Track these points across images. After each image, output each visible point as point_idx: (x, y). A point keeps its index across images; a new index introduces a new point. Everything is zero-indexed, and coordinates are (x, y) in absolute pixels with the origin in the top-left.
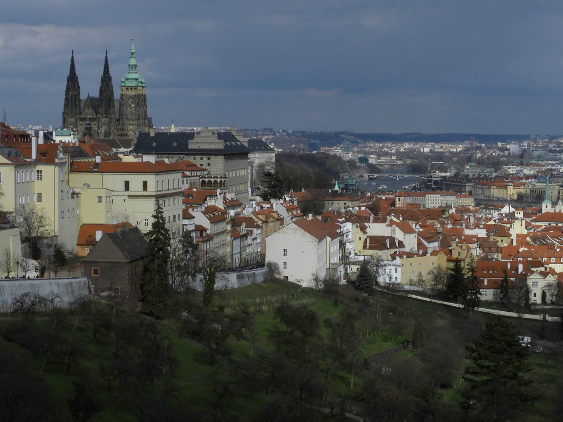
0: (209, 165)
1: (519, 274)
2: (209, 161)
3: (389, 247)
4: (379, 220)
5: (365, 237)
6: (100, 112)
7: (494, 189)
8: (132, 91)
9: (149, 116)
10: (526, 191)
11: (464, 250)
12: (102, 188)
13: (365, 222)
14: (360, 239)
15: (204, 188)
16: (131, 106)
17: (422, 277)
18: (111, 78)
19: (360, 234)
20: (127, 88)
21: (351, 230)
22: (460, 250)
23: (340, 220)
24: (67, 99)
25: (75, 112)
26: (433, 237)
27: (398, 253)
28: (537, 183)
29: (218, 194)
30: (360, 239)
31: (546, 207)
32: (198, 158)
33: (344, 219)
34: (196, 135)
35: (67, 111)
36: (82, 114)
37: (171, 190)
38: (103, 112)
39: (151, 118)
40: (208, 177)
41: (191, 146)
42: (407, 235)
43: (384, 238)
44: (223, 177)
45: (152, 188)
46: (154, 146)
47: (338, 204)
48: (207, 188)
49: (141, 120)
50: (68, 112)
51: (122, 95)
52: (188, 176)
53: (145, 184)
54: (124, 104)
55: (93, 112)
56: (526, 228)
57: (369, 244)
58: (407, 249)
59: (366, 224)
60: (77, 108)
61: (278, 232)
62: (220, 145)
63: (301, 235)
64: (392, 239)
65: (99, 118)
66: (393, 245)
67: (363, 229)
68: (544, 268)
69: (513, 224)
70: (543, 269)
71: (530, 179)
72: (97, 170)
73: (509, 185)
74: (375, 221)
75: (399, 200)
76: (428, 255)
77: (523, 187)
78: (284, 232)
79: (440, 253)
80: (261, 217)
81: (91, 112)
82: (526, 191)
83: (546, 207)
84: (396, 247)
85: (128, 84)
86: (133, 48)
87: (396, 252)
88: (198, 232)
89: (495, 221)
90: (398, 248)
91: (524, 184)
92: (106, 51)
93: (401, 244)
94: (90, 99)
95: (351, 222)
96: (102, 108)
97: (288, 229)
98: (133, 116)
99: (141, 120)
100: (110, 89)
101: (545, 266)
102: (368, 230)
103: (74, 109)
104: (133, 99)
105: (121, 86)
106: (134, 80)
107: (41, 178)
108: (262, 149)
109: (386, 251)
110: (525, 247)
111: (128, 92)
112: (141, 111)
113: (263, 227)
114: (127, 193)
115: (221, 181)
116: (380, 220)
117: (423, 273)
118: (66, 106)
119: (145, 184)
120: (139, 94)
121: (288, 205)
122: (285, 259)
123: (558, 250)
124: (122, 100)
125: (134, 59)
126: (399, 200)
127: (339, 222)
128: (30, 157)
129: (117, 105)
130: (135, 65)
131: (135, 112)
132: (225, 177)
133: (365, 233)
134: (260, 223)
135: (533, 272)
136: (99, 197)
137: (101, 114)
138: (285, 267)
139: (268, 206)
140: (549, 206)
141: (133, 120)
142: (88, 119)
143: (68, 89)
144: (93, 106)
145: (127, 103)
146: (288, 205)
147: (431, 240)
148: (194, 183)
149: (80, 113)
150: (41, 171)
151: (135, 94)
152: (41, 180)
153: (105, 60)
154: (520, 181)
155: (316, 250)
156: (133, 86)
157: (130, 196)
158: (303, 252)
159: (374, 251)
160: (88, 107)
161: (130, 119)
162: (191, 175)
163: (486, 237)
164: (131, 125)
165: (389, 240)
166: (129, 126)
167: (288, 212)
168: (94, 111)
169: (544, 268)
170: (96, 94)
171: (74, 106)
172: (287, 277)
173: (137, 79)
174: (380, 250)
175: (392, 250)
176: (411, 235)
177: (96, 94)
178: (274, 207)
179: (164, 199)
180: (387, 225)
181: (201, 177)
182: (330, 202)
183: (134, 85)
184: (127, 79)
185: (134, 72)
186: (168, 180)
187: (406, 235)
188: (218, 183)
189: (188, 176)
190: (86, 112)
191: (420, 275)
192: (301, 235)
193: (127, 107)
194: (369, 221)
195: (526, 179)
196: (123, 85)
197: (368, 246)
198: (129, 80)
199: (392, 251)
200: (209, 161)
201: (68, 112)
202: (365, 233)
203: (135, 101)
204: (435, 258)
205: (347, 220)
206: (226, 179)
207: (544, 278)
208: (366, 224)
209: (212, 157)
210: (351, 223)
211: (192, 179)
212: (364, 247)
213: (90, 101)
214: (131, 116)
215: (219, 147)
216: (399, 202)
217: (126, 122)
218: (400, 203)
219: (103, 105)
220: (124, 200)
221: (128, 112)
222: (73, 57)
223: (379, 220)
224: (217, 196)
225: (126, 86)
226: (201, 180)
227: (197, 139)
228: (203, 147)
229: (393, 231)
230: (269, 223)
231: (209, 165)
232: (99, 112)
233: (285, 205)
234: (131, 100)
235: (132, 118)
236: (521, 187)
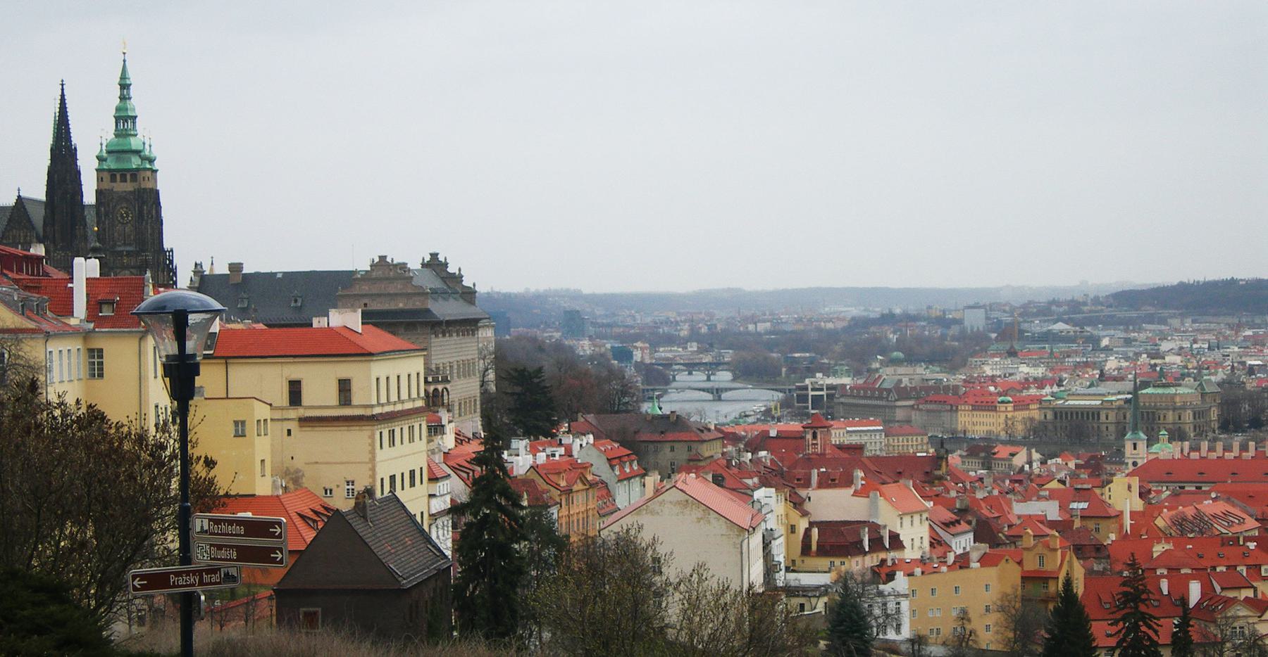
1: (1191, 606)
3: (867, 549)
5: (803, 524)
8: (126, 181)
9: (167, 246)
10: (1045, 416)
12: (227, 398)
13: (800, 486)
14: (793, 529)
17: (969, 620)
18: (75, 149)
19: (795, 514)
22: (1040, 549)
23: (749, 482)
26: (962, 522)
27: (890, 563)
29: (445, 421)
30: (793, 529)
31: (1135, 448)
33: (756, 480)
37: (383, 405)
39: (172, 251)
42: (907, 520)
43: (855, 526)
44: (440, 379)
45: (363, 396)
47: (672, 450)
51: (99, 193)
53: (344, 387)
56: (1141, 495)
58: (910, 554)
59: (803, 493)
63: (699, 520)
64: (875, 528)
66: (877, 544)
67: (798, 504)
68: (1252, 590)
69: (1107, 488)
70: (1249, 593)
71: (1048, 387)
72: (212, 352)
74: (821, 485)
75: (815, 437)
76: (975, 565)
79: (1004, 561)
80: (554, 478)
81: (27, 236)
82: (1045, 416)
83: (1135, 448)
84: (883, 549)
87: (883, 561)
89: (1062, 482)
92: (62, 81)
93: (896, 542)
95: (771, 487)
98: (130, 245)
101: (1255, 584)
102: (808, 506)
107: (101, 369)
110: (1167, 542)
111: (114, 184)
113: (561, 506)
114: (301, 412)
115: (436, 390)
117: (971, 615)
119: (344, 387)
121: (609, 448)
123: (1252, 545)
126: (815, 437)
127: (748, 488)
128: (70, 313)
129: (90, 217)
132: (445, 380)
133: (805, 514)
134: (555, 493)
135: (1230, 602)
136: (236, 423)
139: (562, 450)
140: (1142, 446)
141: (129, 254)
146: (609, 448)
147: (959, 528)
150: (101, 351)
151: (132, 189)
152: (101, 375)
153: (60, 104)
154: (1025, 393)
155: (739, 556)
157: (305, 421)
159: (832, 560)
163: (1060, 519)
167: (612, 467)
169: (1252, 590)
174: (846, 556)
175: (875, 555)
178: (575, 454)
179: (391, 426)
180: (856, 494)
182: (651, 447)
186: (398, 377)
191: (964, 616)
192: (699, 520)
194: (807, 484)
197: (814, 547)
199: (871, 561)
202: (805, 514)
204: (992, 572)
205: (765, 483)
206: (448, 386)
207: (1259, 614)
208: (803, 493)
210: (773, 490)
212: (806, 549)
214: (125, 244)
215: (417, 303)
216: (815, 442)
218: (817, 444)
220: (289, 432)
221: (116, 234)
224: (443, 426)
225: (110, 170)
229: (874, 508)
230: (575, 494)
233: (603, 449)
235: (128, 248)
236: (1032, 407)
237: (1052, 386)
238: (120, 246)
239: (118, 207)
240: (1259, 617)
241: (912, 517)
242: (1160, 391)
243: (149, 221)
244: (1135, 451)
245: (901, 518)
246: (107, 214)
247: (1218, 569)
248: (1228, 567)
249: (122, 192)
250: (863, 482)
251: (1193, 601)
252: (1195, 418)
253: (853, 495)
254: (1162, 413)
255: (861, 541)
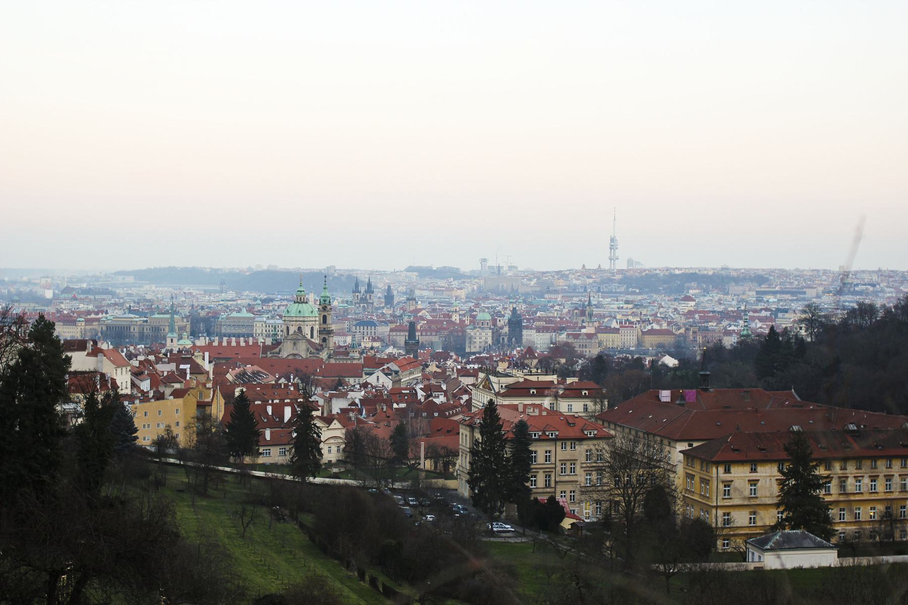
7: (60, 327)
10: (102, 328)
11: (209, 389)
28: (114, 318)
31: (172, 342)
42: (119, 370)
64: (103, 375)
71: (100, 313)
73: (80, 321)
77: (97, 323)
79: (187, 394)
82: (102, 328)
83: (172, 342)
91: (98, 320)
154: (89, 317)
176: (124, 369)
180: (88, 355)
195: (95, 314)
207: (327, 426)
236: (94, 323)
237: (102, 314)
240: (327, 427)
241: (122, 369)
242: (162, 316)
244: (172, 344)
245: (116, 370)
247: (275, 401)
248: (280, 400)
250: (93, 348)
251: (286, 419)
252: (179, 330)
253: (86, 356)
254: (162, 328)
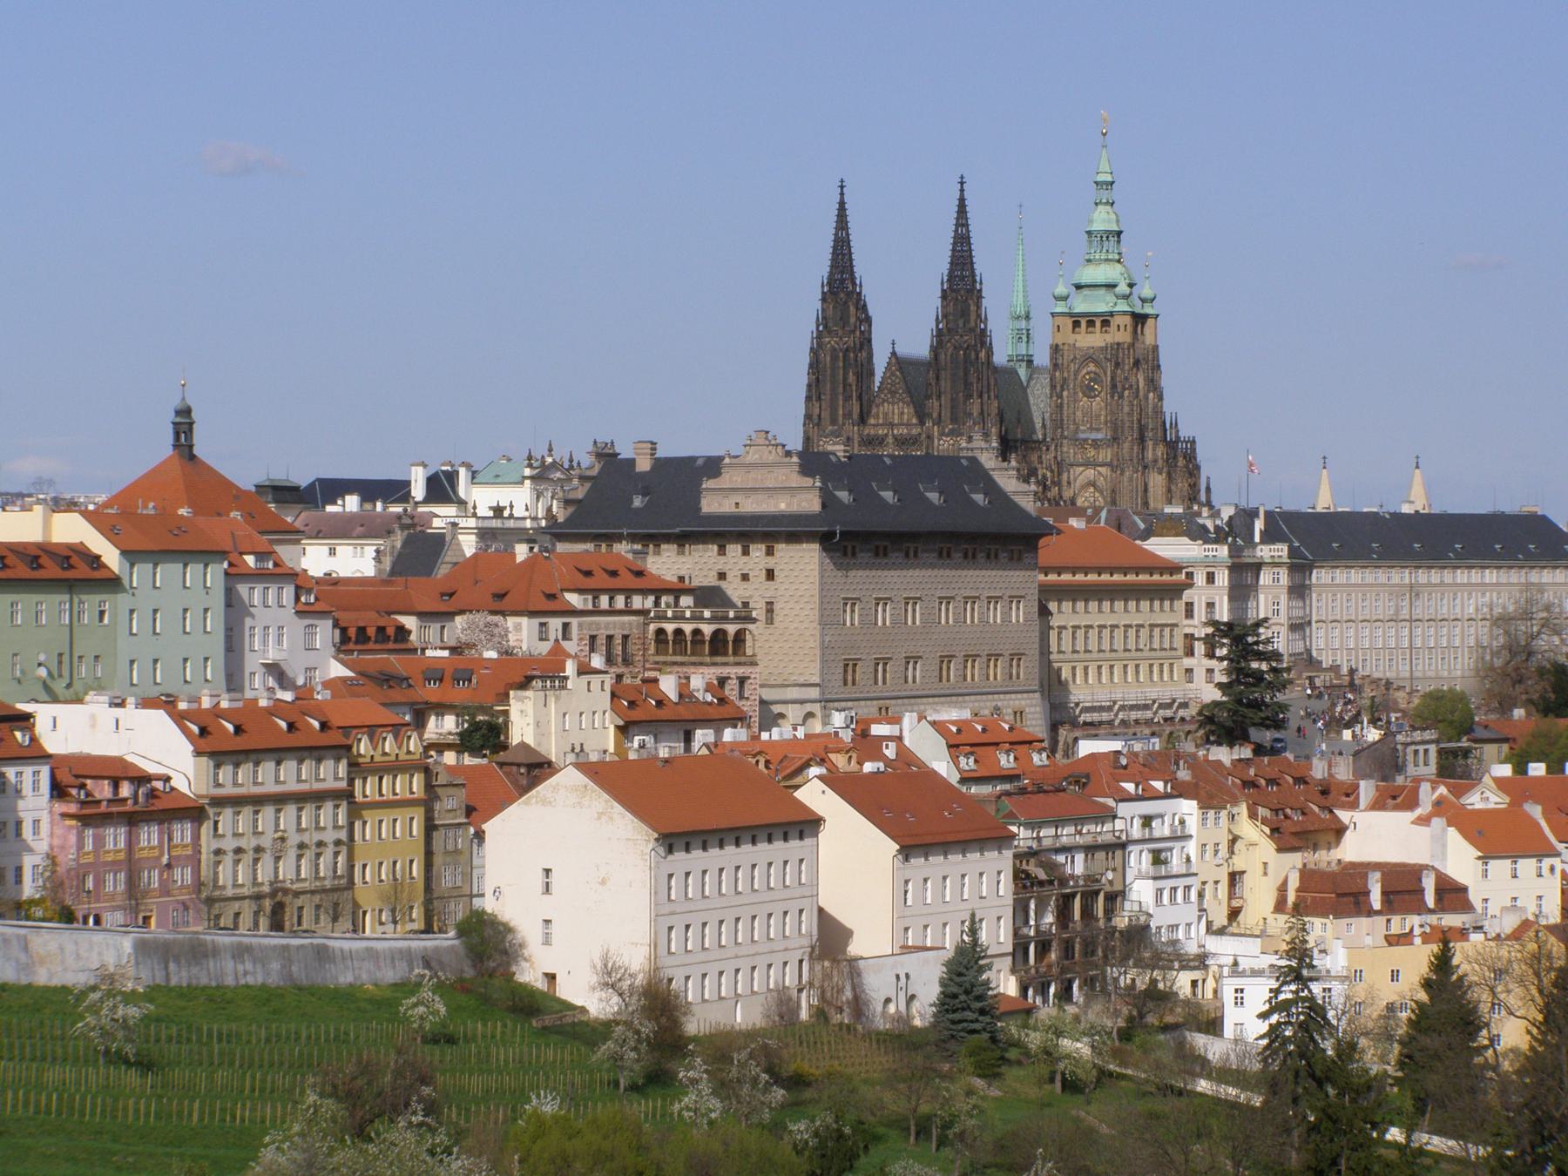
0: (770, 574)
2: (771, 562)
4: (1394, 798)
6: (935, 415)
15: (719, 659)
16: (1089, 392)
20: (1076, 324)
21: (1193, 832)
24: (815, 366)
25: (844, 415)
32: (734, 549)
34: (727, 460)
35: (817, 411)
36: (872, 421)
38: (946, 414)
40: (676, 618)
41: (712, 505)
42: (1500, 867)
46: (638, 509)
48: (669, 659)
49: (1126, 445)
50: (819, 416)
51: (1056, 349)
52: (574, 612)
54: (1065, 380)
55: (908, 411)
57: (1298, 890)
60: (851, 397)
61: (526, 803)
62: (809, 502)
65: (929, 437)
74: (1378, 805)
78: (545, 802)
81: (902, 413)
85: (1081, 305)
86: (1105, 166)
88: (106, 782)
90: (1431, 911)
94: (899, 363)
96: (939, 397)
97: (555, 788)
98: (1098, 430)
99: (1126, 445)
100: (972, 324)
103: (841, 402)
104: (1095, 362)
105: (1053, 314)
106: (1102, 291)
108: (1455, 551)
109: (1363, 922)
111: (1077, 337)
112: (1126, 409)
116: (1399, 800)
118: (815, 391)
120: (1118, 344)
122: (547, 908)
124: (1056, 366)
125: (1108, 208)
130: (1109, 233)
131: (1103, 413)
137: (938, 422)
138: (547, 941)
141: (1096, 444)
142: (890, 440)
143: (826, 326)
144: (908, 391)
145: (1076, 379)
148: (610, 638)
149: (863, 420)
151: (1103, 344)
156: (1097, 315)
158: (603, 882)
160: (893, 393)
161: (1086, 440)
162: (590, 607)
164: (1088, 464)
165: (1378, 875)
166: (1081, 469)
168: (912, 411)
170: (918, 345)
171: (841, 389)
172: (551, 978)
173: (1111, 286)
177: (918, 345)
181: (652, 614)
183: (1102, 308)
184: (1079, 287)
185: (1107, 260)
187: (1494, 865)
188: (703, 642)
189: (574, 612)
190: (886, 414)
193: (1076, 393)
194: (1354, 806)
196: (1058, 310)
198: (1086, 292)
200: (771, 562)
201: (819, 416)
203: (1105, 374)
209: (780, 548)
211: (598, 624)
213: (900, 369)
214: (1091, 429)
215: (804, 504)
217: (1069, 452)
219: (945, 384)
221: (1079, 414)
222: (842, 204)
223: (1394, 798)
225: (1071, 315)
226: (652, 627)
227: (726, 480)
228: (752, 505)
231: (770, 574)
232: (930, 415)
234: (1092, 367)
235: (1094, 435)
238: (1084, 431)
239: (1085, 371)
243: (1126, 393)
246: (1065, 380)
249: (1088, 348)
253: (1413, 823)
255: (1367, 893)
